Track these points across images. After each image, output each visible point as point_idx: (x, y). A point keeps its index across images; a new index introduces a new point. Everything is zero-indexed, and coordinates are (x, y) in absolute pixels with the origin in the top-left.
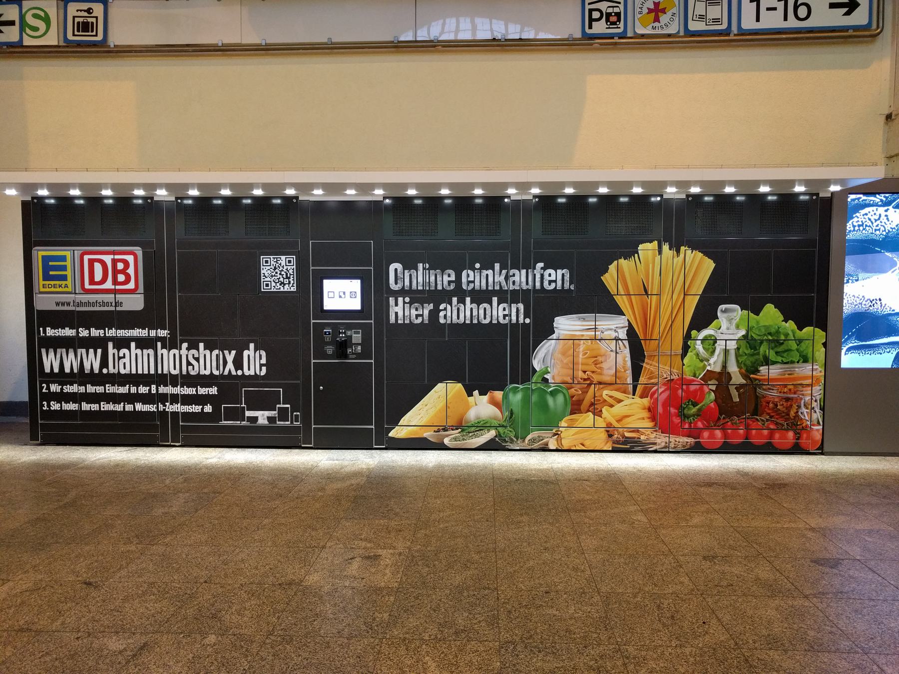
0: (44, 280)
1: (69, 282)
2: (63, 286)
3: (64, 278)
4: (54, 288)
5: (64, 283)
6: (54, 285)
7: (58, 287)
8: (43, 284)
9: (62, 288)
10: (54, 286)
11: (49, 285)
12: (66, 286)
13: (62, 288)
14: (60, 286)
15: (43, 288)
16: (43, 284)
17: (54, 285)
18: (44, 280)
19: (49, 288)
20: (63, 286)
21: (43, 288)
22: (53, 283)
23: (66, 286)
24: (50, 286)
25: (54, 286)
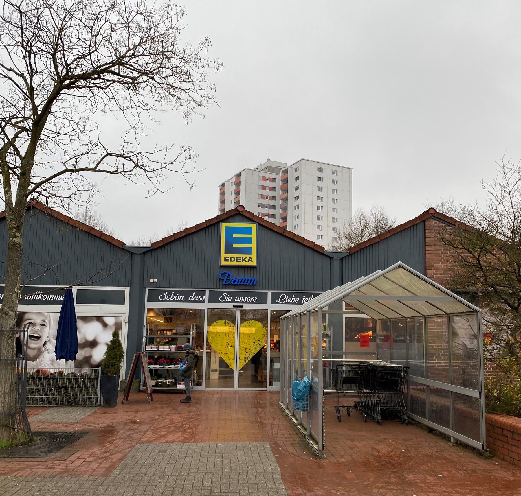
0: (226, 252)
1: (254, 256)
2: (247, 260)
3: (248, 251)
4: (237, 261)
5: (248, 256)
6: (237, 258)
7: (241, 260)
8: (225, 258)
9: (246, 261)
10: (238, 259)
11: (231, 258)
12: (250, 260)
13: (246, 261)
14: (244, 260)
15: (225, 261)
16: (225, 258)
17: (237, 258)
18: (226, 252)
19: (231, 261)
20: (247, 260)
21: (225, 261)
22: (235, 256)
23: (250, 260)
24: (233, 259)
25: (238, 259)
